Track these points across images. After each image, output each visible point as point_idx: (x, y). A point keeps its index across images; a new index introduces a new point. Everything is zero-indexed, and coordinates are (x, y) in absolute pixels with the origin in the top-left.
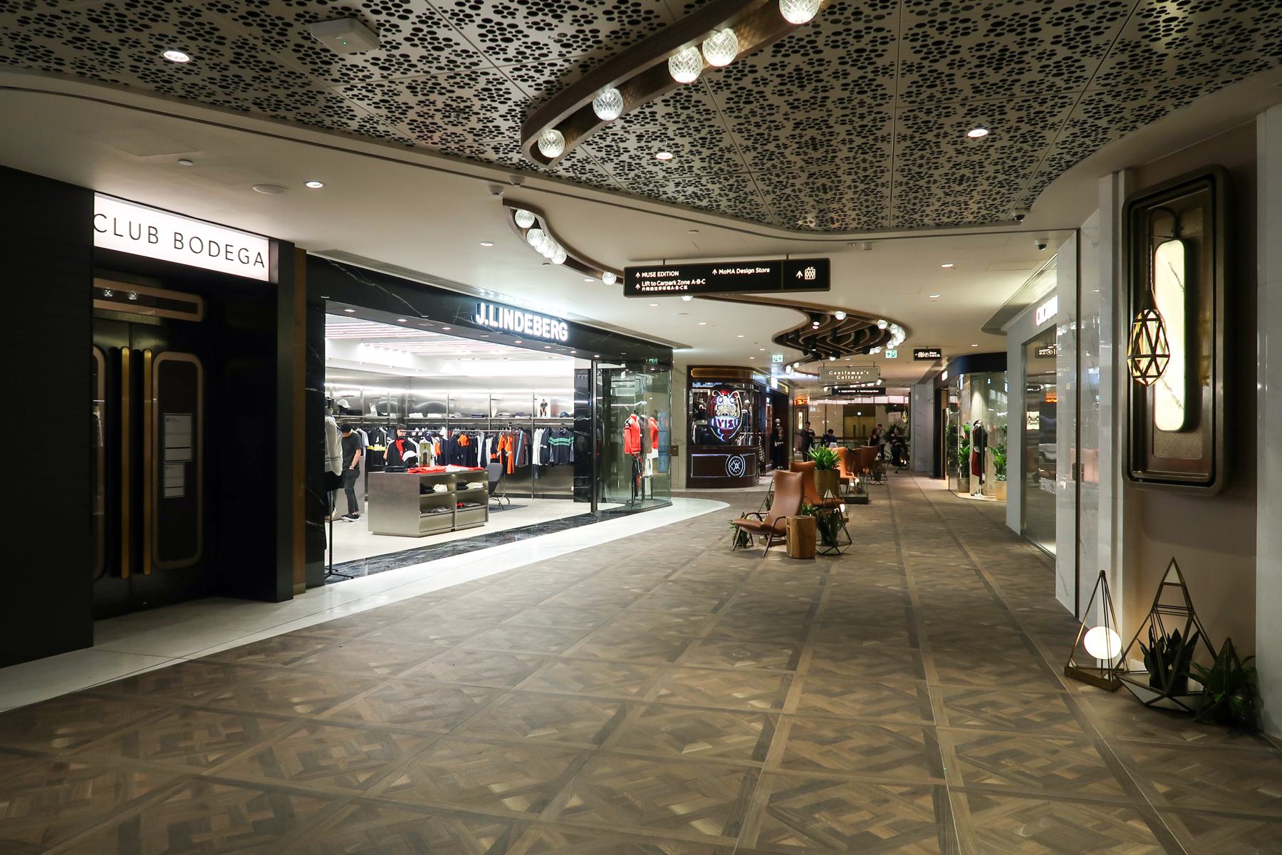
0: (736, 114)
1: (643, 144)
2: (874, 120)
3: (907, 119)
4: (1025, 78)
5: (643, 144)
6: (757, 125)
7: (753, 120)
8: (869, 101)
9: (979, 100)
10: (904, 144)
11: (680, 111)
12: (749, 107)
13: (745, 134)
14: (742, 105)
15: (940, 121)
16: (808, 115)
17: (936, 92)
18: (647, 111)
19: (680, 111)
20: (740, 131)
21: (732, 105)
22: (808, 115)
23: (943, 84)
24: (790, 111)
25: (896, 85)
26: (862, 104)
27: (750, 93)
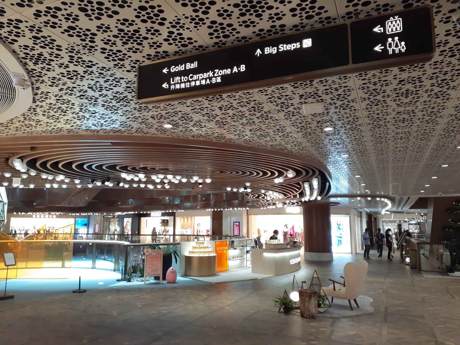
0: (290, 120)
1: (252, 132)
2: (353, 119)
3: (369, 117)
4: (421, 100)
5: (252, 132)
6: (300, 123)
7: (298, 121)
8: (349, 112)
9: (401, 109)
10: (370, 126)
11: (265, 121)
12: (294, 117)
13: (296, 127)
14: (291, 117)
15: (384, 117)
16: (322, 118)
17: (380, 107)
18: (251, 121)
19: (265, 121)
20: (293, 126)
21: (286, 117)
22: (322, 118)
23: (382, 104)
24: (313, 118)
25: (361, 106)
26: (346, 113)
27: (293, 113)
